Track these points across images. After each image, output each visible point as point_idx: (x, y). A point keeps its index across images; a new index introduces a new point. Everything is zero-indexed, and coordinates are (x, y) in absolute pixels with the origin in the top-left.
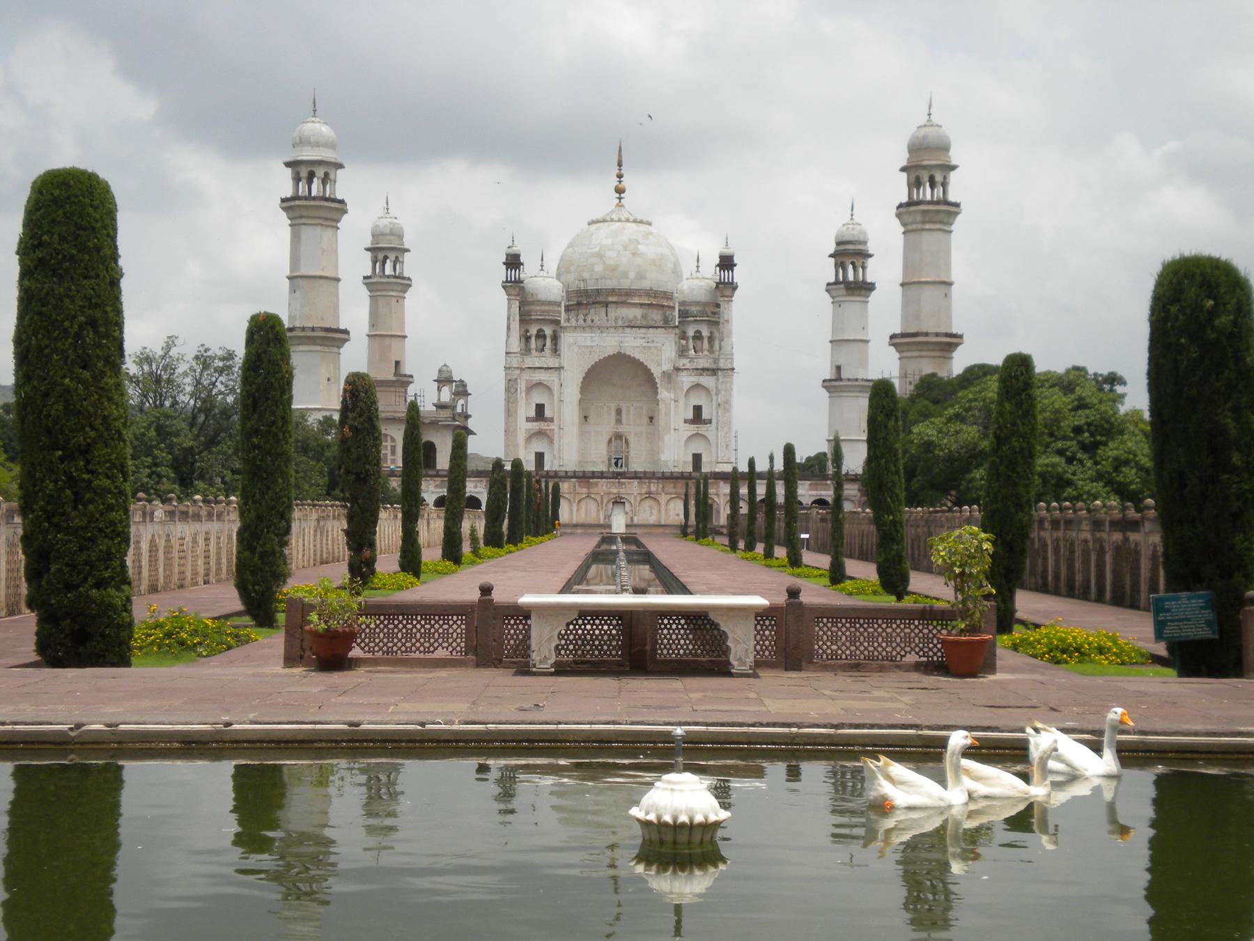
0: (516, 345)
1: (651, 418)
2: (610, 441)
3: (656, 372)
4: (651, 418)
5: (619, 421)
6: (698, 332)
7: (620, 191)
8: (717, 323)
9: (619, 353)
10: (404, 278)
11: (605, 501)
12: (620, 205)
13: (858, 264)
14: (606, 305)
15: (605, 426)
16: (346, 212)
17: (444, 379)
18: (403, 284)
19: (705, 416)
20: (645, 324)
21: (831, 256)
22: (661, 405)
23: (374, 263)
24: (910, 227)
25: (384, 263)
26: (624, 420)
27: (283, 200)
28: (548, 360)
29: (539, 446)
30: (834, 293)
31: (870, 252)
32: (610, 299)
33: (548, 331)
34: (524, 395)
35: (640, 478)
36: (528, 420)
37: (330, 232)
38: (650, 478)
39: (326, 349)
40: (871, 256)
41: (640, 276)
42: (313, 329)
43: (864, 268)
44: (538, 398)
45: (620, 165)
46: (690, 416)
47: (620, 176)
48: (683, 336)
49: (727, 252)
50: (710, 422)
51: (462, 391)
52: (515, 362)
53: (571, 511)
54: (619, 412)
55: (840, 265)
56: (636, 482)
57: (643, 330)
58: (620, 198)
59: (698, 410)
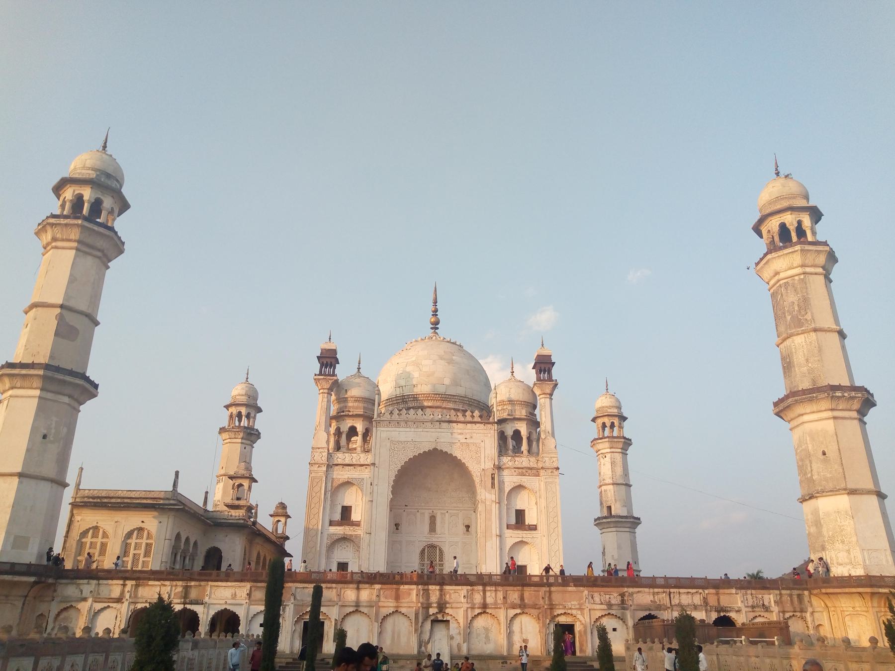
0: (323, 439)
1: (468, 527)
3: (475, 469)
4: (468, 527)
5: (433, 528)
6: (517, 434)
8: (537, 424)
9: (435, 449)
10: (253, 429)
11: (420, 620)
13: (616, 424)
14: (423, 408)
15: (418, 535)
16: (121, 252)
17: (243, 479)
18: (251, 435)
19: (529, 520)
20: (461, 418)
22: (481, 507)
23: (231, 416)
24: (782, 275)
25: (240, 421)
27: (39, 224)
29: (342, 554)
30: (600, 446)
31: (625, 415)
32: (426, 404)
33: (360, 427)
34: (329, 495)
35: (471, 584)
36: (331, 523)
37: (89, 262)
38: (484, 585)
39: (49, 395)
40: (625, 419)
41: (455, 383)
42: (32, 366)
43: (621, 427)
45: (435, 302)
46: (513, 521)
47: (435, 312)
48: (502, 436)
49: (545, 352)
50: (533, 528)
51: (282, 511)
52: (322, 457)
53: (371, 631)
56: (463, 590)
57: (460, 425)
59: (520, 514)
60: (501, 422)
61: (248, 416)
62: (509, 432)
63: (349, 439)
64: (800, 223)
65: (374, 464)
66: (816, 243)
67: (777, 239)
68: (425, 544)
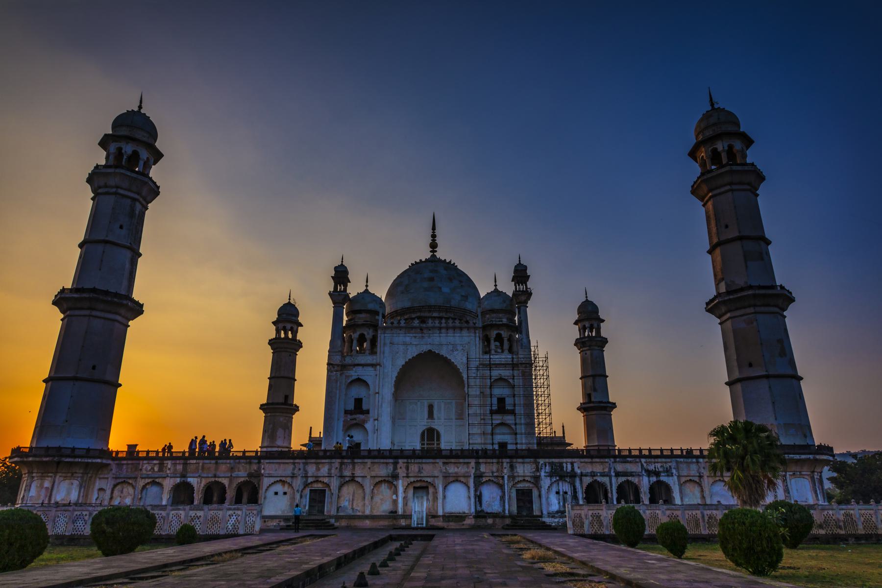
2: (423, 434)
7: (434, 246)
12: (433, 256)
13: (595, 325)
21: (576, 323)
23: (278, 331)
26: (435, 416)
28: (368, 359)
44: (357, 391)
45: (434, 228)
47: (434, 236)
48: (486, 340)
52: (337, 359)
54: (431, 408)
55: (583, 330)
56: (440, 462)
58: (433, 251)
59: (501, 401)
60: (484, 328)
61: (291, 329)
62: (493, 333)
63: (361, 345)
64: (731, 147)
65: (379, 364)
66: (746, 164)
67: (708, 162)
68: (425, 428)
